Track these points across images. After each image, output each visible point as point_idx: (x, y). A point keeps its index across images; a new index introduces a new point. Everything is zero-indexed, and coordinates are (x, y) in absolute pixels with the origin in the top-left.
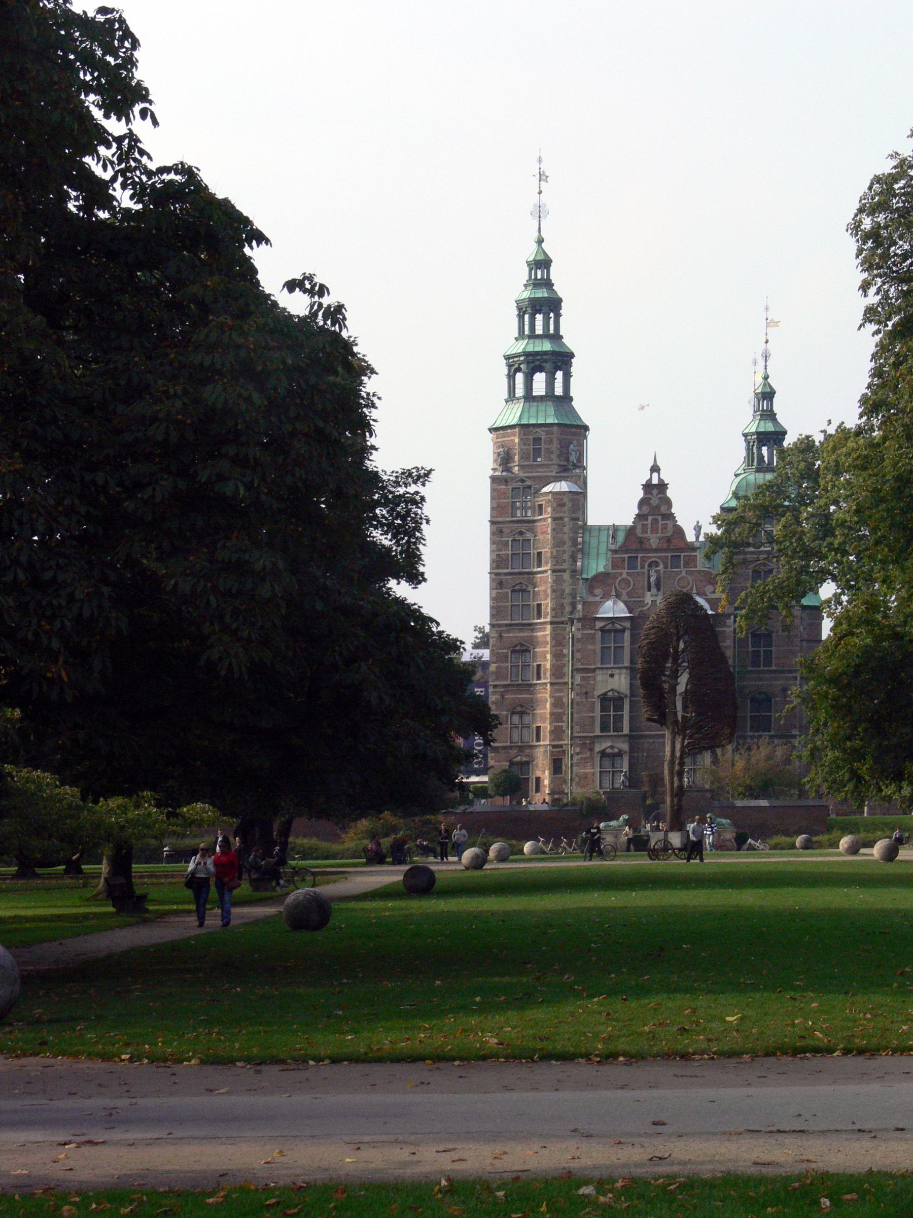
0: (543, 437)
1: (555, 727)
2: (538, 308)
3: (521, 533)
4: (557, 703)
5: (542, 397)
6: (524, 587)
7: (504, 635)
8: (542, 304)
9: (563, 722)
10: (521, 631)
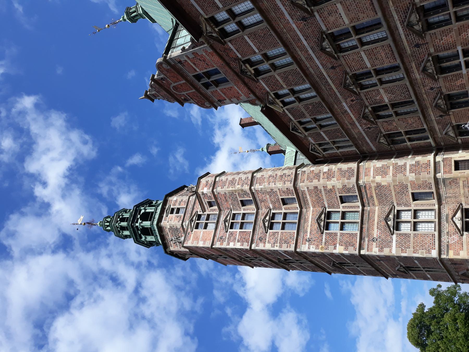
0: (172, 207)
1: (411, 171)
2: (119, 219)
3: (225, 221)
4: (383, 172)
6: (267, 218)
7: (308, 236)
9: (405, 165)
10: (306, 220)
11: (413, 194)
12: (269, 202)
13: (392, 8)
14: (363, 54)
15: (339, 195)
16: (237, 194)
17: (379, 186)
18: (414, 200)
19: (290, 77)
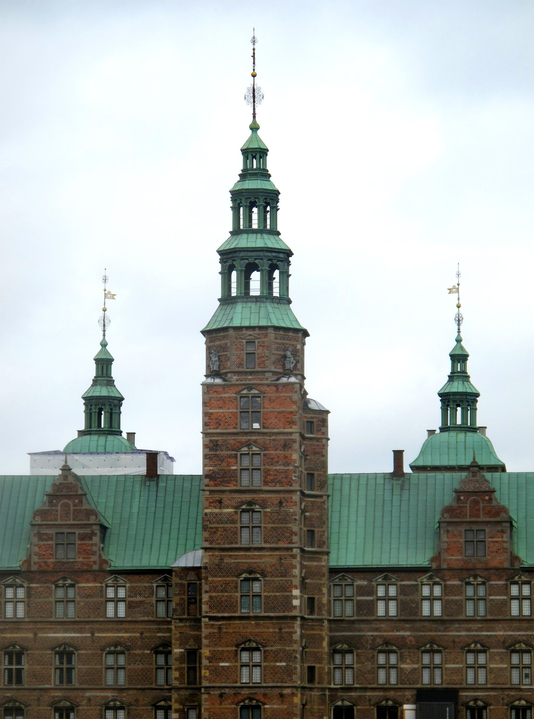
5: (256, 297)
8: (255, 197)
11: (314, 667)
12: (313, 514)
13: (492, 693)
14: (461, 666)
15: (316, 598)
16: (322, 473)
17: (322, 639)
18: (309, 667)
19: (456, 607)
